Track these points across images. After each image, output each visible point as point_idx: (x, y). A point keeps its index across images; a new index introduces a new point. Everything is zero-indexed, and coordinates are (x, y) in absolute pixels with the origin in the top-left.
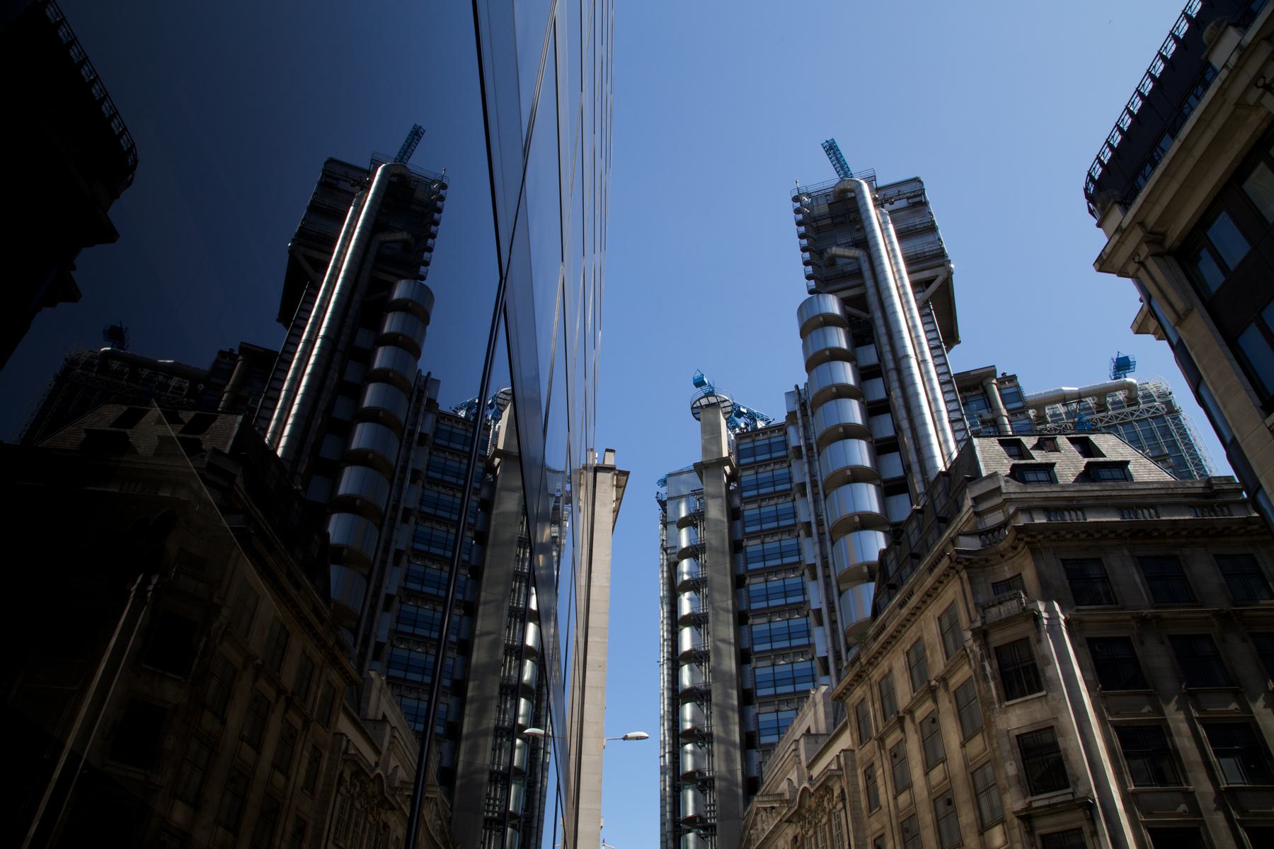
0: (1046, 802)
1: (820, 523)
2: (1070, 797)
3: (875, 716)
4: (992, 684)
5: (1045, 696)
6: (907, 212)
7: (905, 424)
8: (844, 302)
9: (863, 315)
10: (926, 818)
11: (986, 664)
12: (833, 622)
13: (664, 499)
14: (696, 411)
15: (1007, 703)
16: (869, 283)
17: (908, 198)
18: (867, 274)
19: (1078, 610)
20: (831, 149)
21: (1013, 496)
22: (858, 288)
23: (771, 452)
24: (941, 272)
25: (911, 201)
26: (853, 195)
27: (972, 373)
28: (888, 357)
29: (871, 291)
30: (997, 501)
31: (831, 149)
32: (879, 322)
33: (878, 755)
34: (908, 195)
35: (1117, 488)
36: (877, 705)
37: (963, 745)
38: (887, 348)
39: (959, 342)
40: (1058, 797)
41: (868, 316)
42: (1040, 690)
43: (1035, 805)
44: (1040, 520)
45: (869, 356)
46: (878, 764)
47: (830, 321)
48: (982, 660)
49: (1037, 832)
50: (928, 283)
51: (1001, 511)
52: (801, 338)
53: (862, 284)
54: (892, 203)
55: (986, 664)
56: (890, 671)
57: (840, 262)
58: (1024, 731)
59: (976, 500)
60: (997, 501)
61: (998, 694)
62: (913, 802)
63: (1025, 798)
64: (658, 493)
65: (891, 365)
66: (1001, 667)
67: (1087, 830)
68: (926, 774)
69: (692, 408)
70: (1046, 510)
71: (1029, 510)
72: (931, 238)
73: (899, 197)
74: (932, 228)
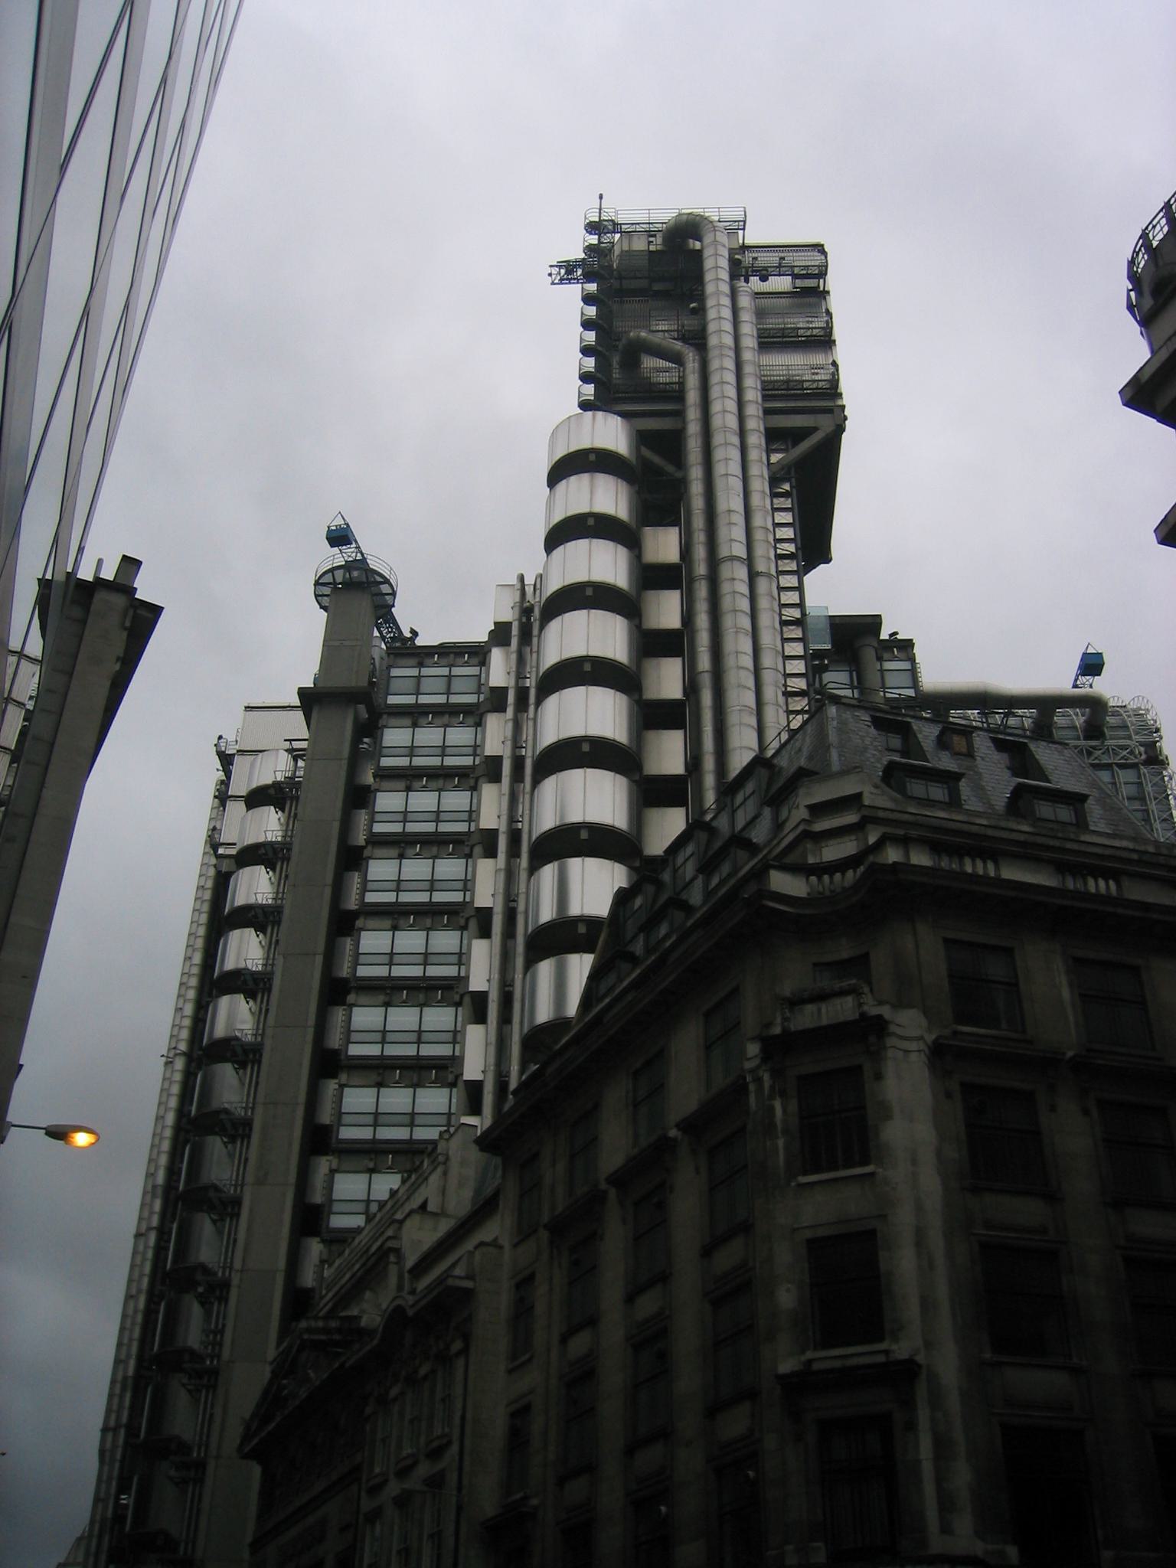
0: (838, 1364)
1: (515, 837)
2: (881, 1359)
4: (781, 1143)
5: (872, 1174)
6: (784, 302)
7: (706, 681)
8: (641, 438)
9: (670, 468)
10: (613, 1377)
11: (778, 1105)
12: (505, 1019)
15: (803, 1179)
16: (693, 414)
17: (795, 276)
18: (692, 396)
19: (955, 1033)
21: (881, 814)
22: (667, 419)
23: (448, 693)
24: (825, 423)
25: (799, 283)
26: (698, 245)
28: (700, 552)
29: (693, 428)
30: (850, 818)
32: (696, 488)
34: (796, 270)
35: (1060, 835)
37: (707, 1251)
38: (700, 538)
39: (827, 559)
40: (858, 1354)
41: (679, 475)
42: (865, 1162)
43: (816, 1366)
44: (920, 858)
45: (664, 545)
48: (771, 1097)
50: (795, 436)
51: (853, 837)
52: (548, 486)
53: (680, 414)
54: (764, 279)
55: (778, 1105)
57: (649, 362)
58: (821, 1232)
59: (818, 810)
60: (850, 818)
63: (803, 1352)
64: (220, 737)
65: (701, 569)
68: (630, 1299)
69: (317, 583)
70: (936, 847)
71: (904, 842)
72: (818, 358)
73: (780, 270)
74: (824, 341)
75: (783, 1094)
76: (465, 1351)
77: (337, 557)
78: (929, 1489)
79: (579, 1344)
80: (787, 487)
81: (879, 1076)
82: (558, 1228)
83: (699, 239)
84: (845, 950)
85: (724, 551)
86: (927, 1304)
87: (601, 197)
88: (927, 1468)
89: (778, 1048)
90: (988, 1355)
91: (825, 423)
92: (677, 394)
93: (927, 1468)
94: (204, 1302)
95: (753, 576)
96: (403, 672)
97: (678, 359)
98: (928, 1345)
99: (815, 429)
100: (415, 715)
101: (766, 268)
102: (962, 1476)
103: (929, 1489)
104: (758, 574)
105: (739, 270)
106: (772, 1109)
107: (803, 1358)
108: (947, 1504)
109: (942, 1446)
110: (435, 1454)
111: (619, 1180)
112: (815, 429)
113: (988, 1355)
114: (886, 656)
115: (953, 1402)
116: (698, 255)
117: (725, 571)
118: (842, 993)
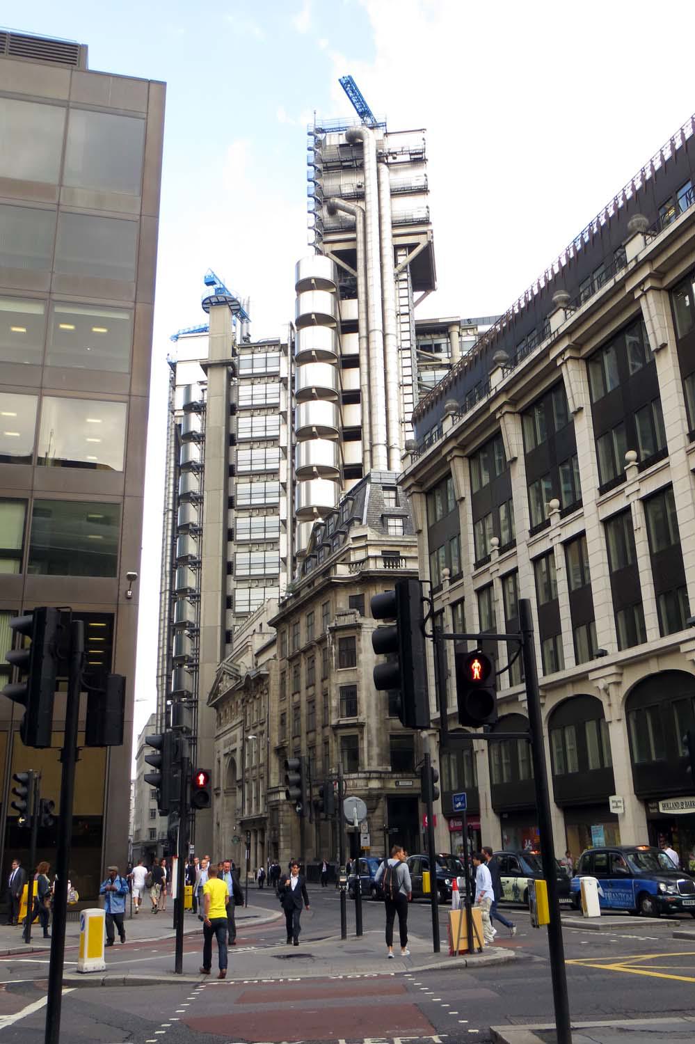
2: (356, 721)
3: (289, 644)
4: (334, 658)
9: (351, 271)
11: (333, 646)
13: (173, 362)
14: (205, 306)
20: (348, 85)
25: (413, 157)
26: (360, 141)
27: (441, 321)
30: (363, 543)
31: (348, 85)
33: (288, 667)
36: (291, 638)
39: (435, 290)
43: (341, 723)
45: (351, 309)
46: (287, 673)
47: (321, 284)
49: (339, 735)
50: (411, 247)
55: (333, 646)
56: (299, 622)
57: (341, 213)
59: (354, 539)
60: (363, 543)
61: (336, 665)
62: (299, 701)
63: (338, 718)
64: (168, 355)
66: (340, 651)
67: (359, 737)
69: (203, 303)
73: (402, 152)
75: (335, 644)
76: (267, 693)
77: (211, 291)
78: (366, 755)
79: (297, 697)
80: (404, 276)
81: (359, 640)
82: (291, 660)
83: (362, 138)
84: (357, 592)
85: (371, 328)
86: (369, 707)
87: (315, 113)
88: (366, 750)
89: (333, 630)
90: (388, 717)
91: (423, 241)
92: (352, 228)
93: (366, 750)
94: (191, 637)
95: (384, 336)
96: (245, 357)
97: (353, 213)
98: (368, 717)
99: (418, 244)
100: (253, 378)
101: (395, 153)
102: (375, 751)
103: (366, 755)
104: (388, 334)
105: (380, 158)
106: (332, 648)
107: (339, 719)
108: (370, 758)
109: (370, 743)
110: (262, 724)
111: (304, 651)
112: (418, 244)
113: (388, 717)
114: (464, 333)
115: (374, 732)
116: (360, 146)
117: (372, 335)
118: (352, 614)
